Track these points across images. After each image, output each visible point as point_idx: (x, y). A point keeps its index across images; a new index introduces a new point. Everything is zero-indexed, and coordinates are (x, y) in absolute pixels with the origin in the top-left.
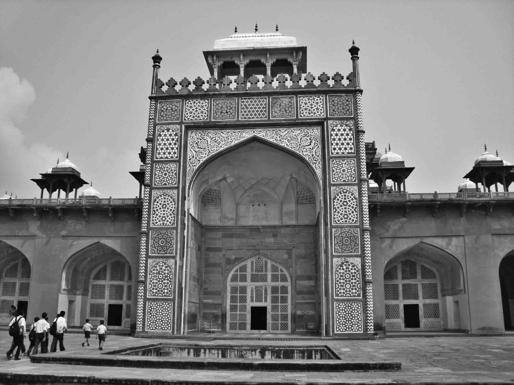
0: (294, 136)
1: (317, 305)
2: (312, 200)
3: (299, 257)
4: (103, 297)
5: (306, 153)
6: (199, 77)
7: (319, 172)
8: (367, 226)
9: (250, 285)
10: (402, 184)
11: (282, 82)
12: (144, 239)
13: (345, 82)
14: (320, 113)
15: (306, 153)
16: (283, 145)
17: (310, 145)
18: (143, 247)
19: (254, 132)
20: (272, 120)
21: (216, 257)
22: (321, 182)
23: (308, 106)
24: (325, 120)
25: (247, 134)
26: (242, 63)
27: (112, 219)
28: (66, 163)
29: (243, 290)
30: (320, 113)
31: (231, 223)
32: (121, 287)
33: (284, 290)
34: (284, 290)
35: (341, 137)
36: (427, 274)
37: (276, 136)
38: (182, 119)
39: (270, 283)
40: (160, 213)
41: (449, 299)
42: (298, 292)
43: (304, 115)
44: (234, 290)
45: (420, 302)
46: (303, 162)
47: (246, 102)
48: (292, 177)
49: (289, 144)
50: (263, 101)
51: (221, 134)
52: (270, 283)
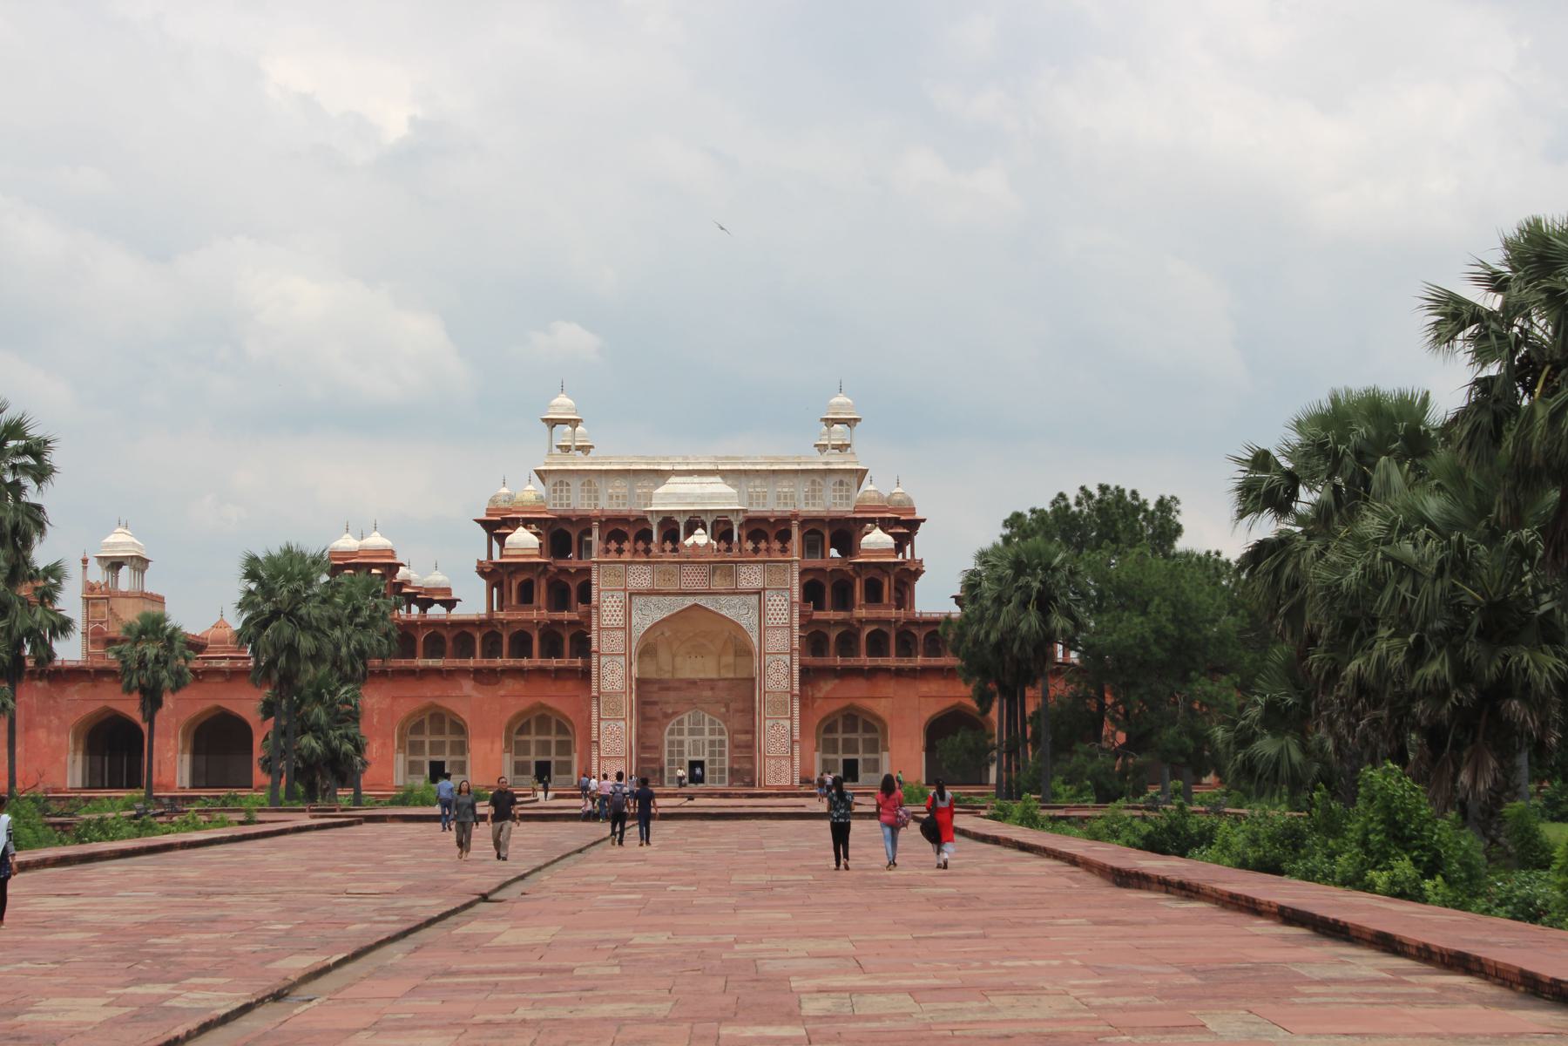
1: (752, 760)
2: (749, 653)
3: (737, 711)
4: (527, 752)
7: (755, 640)
8: (796, 692)
9: (687, 739)
12: (595, 702)
18: (595, 710)
21: (653, 711)
25: (689, 601)
28: (376, 541)
29: (681, 743)
31: (667, 676)
32: (549, 743)
33: (722, 743)
34: (722, 743)
36: (869, 728)
39: (707, 737)
40: (609, 678)
41: (885, 755)
42: (735, 746)
44: (671, 743)
45: (860, 757)
47: (687, 569)
52: (707, 737)
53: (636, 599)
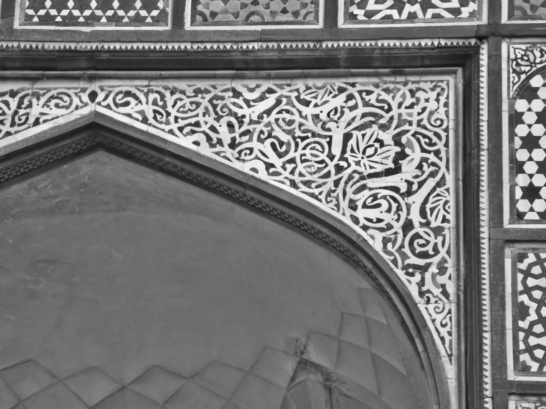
0: (310, 125)
5: (373, 214)
7: (440, 318)
15: (373, 214)
16: (245, 168)
17: (397, 170)
19: (93, 96)
20: (195, 37)
22: (450, 371)
24: (481, 39)
37: (211, 121)
43: (369, 14)
46: (357, 264)
48: (304, 364)
49: (278, 162)
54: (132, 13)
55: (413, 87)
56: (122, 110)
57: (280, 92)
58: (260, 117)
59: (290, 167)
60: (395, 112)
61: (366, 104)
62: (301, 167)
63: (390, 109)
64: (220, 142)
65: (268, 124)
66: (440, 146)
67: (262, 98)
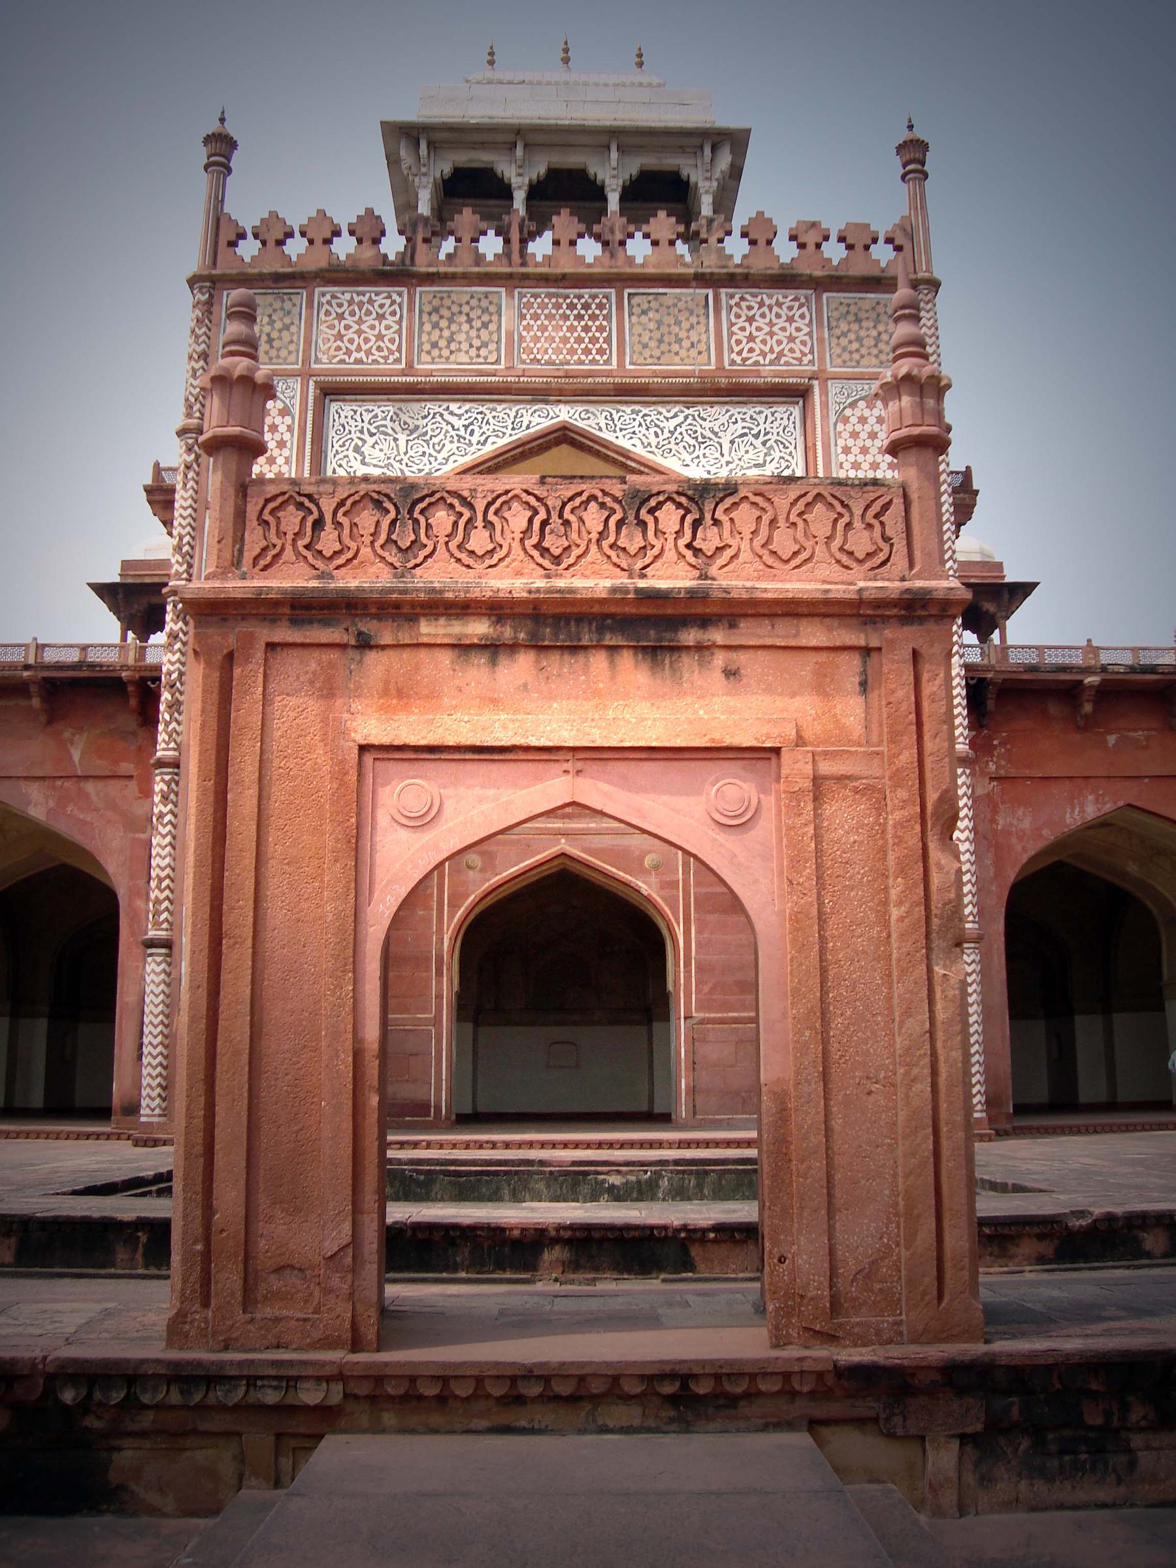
0: (708, 434)
6: (370, 212)
10: (997, 631)
11: (664, 243)
13: (882, 254)
14: (798, 355)
23: (759, 329)
26: (519, 176)
27: (43, 718)
30: (798, 355)
35: (868, 443)
37: (643, 430)
38: (306, 361)
43: (744, 360)
49: (688, 458)
50: (601, 306)
51: (446, 416)
53: (341, 412)
54: (590, 357)
55: (773, 410)
56: (585, 422)
57: (687, 412)
58: (675, 429)
59: (696, 461)
60: (762, 427)
61: (743, 420)
62: (703, 461)
63: (758, 425)
64: (649, 444)
65: (681, 433)
66: (792, 448)
67: (676, 415)
